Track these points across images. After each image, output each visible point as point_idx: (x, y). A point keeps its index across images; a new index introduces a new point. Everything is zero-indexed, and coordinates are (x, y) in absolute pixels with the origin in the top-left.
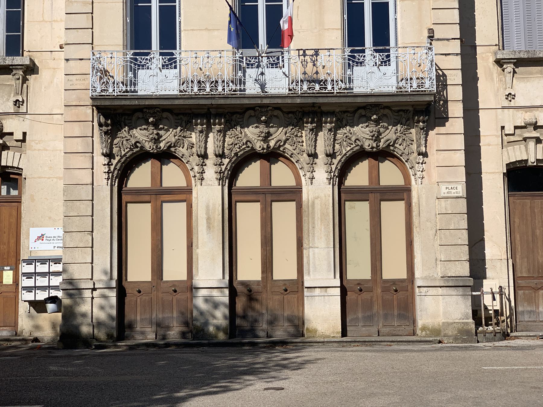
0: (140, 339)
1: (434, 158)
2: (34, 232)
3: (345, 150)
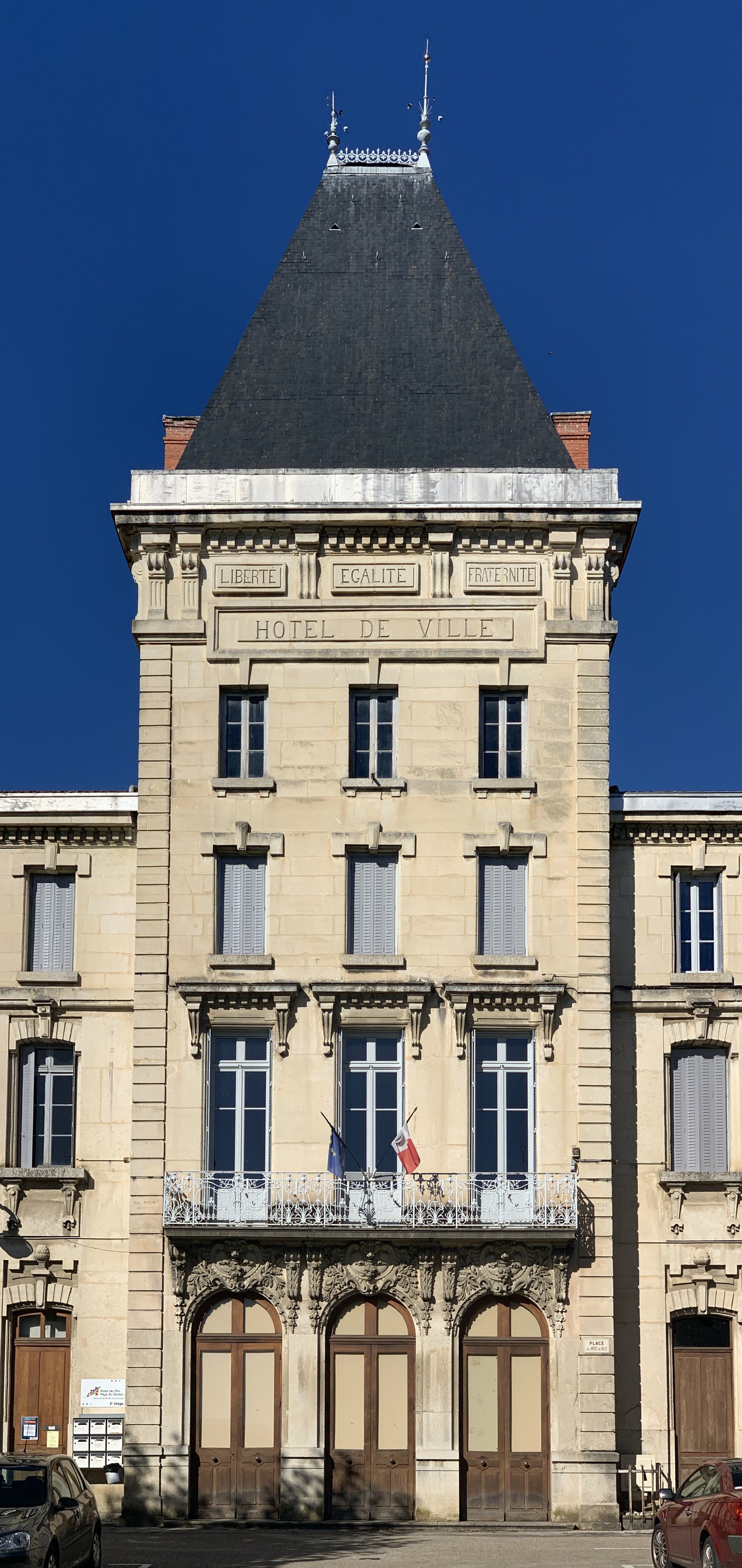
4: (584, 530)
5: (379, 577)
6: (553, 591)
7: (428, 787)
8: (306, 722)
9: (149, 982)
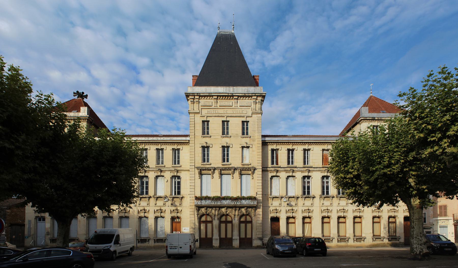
2: (183, 228)
3: (240, 214)
4: (257, 96)
6: (253, 106)
7: (234, 137)
8: (215, 126)
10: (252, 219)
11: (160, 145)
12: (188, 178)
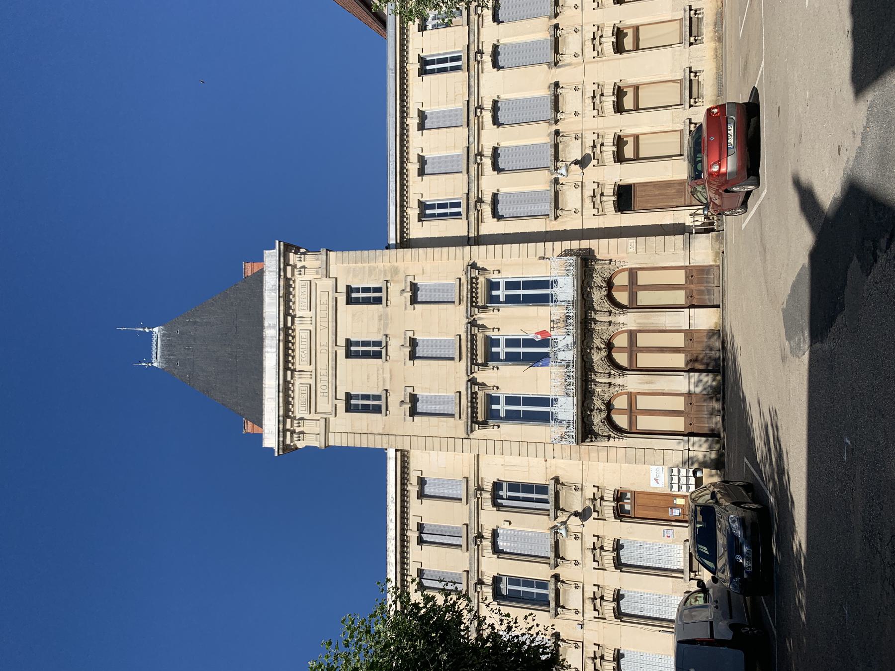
0: (720, 425)
1: (612, 256)
2: (653, 484)
3: (607, 305)
4: (287, 264)
5: (304, 347)
6: (309, 276)
7: (386, 326)
8: (360, 377)
9: (466, 447)
10: (623, 270)
11: (409, 534)
12: (499, 459)
